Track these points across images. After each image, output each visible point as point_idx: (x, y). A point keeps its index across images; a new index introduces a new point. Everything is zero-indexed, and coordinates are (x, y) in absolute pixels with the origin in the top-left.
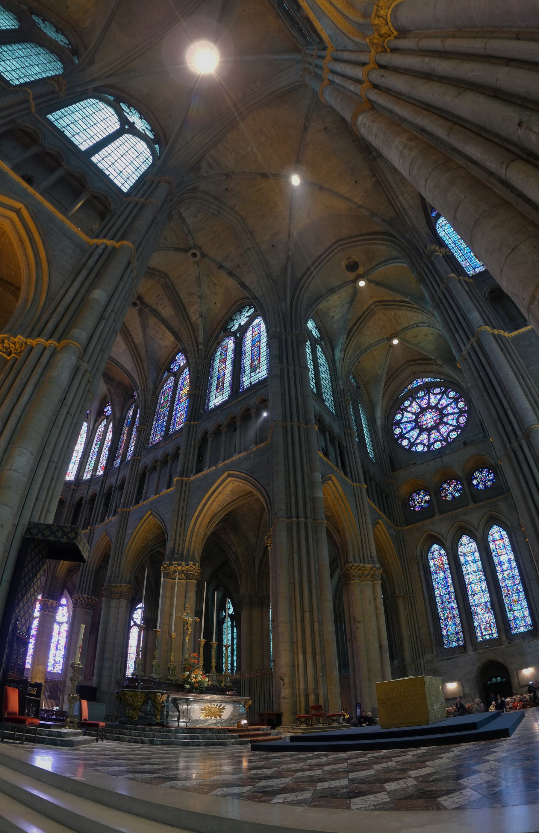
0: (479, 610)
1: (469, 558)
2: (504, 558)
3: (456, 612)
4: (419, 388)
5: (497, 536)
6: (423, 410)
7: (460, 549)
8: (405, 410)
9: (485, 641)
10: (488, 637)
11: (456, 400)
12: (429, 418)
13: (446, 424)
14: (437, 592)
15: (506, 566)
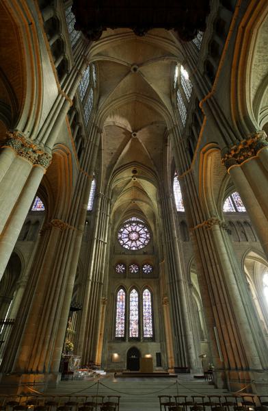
0: (133, 322)
1: (134, 299)
2: (147, 304)
3: (124, 321)
4: (134, 222)
5: (147, 294)
6: (133, 232)
7: (131, 295)
8: (125, 228)
9: (133, 338)
10: (134, 336)
11: (146, 233)
12: (134, 236)
13: (140, 241)
14: (117, 310)
15: (147, 307)
